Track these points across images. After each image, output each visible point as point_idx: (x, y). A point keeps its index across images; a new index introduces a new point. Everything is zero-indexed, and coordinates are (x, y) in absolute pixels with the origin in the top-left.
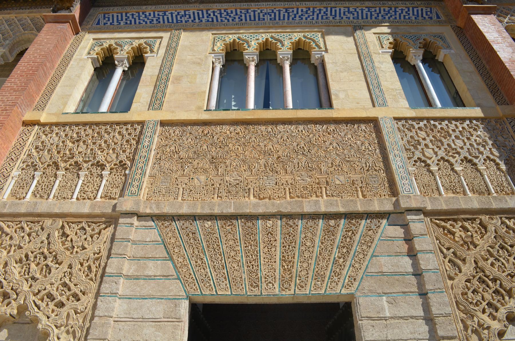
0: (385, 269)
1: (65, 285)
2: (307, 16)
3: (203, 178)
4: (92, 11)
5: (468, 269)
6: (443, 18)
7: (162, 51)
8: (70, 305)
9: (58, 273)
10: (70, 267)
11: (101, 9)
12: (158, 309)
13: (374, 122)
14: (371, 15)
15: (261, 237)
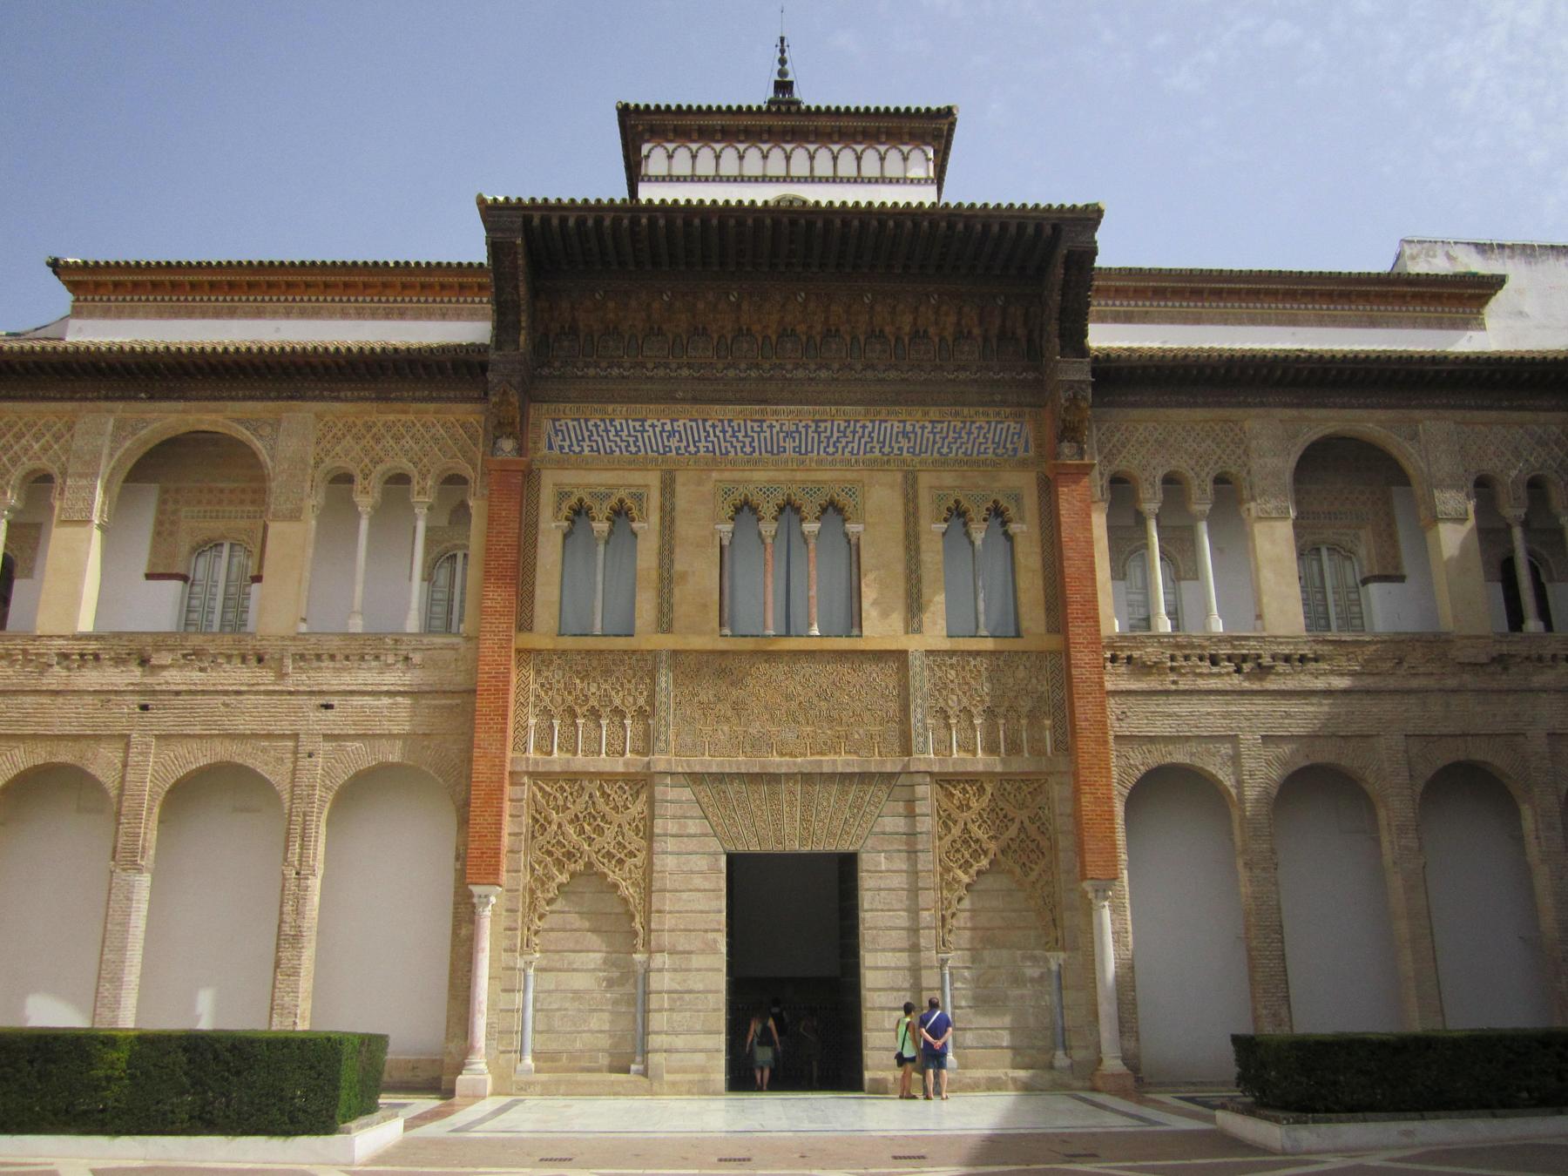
0: (887, 829)
1: (619, 843)
2: (844, 441)
3: (726, 728)
4: (532, 412)
5: (956, 831)
6: (1031, 453)
7: (655, 518)
8: (630, 862)
9: (610, 832)
10: (620, 826)
11: (545, 406)
12: (702, 863)
13: (901, 656)
14: (934, 442)
15: (784, 796)
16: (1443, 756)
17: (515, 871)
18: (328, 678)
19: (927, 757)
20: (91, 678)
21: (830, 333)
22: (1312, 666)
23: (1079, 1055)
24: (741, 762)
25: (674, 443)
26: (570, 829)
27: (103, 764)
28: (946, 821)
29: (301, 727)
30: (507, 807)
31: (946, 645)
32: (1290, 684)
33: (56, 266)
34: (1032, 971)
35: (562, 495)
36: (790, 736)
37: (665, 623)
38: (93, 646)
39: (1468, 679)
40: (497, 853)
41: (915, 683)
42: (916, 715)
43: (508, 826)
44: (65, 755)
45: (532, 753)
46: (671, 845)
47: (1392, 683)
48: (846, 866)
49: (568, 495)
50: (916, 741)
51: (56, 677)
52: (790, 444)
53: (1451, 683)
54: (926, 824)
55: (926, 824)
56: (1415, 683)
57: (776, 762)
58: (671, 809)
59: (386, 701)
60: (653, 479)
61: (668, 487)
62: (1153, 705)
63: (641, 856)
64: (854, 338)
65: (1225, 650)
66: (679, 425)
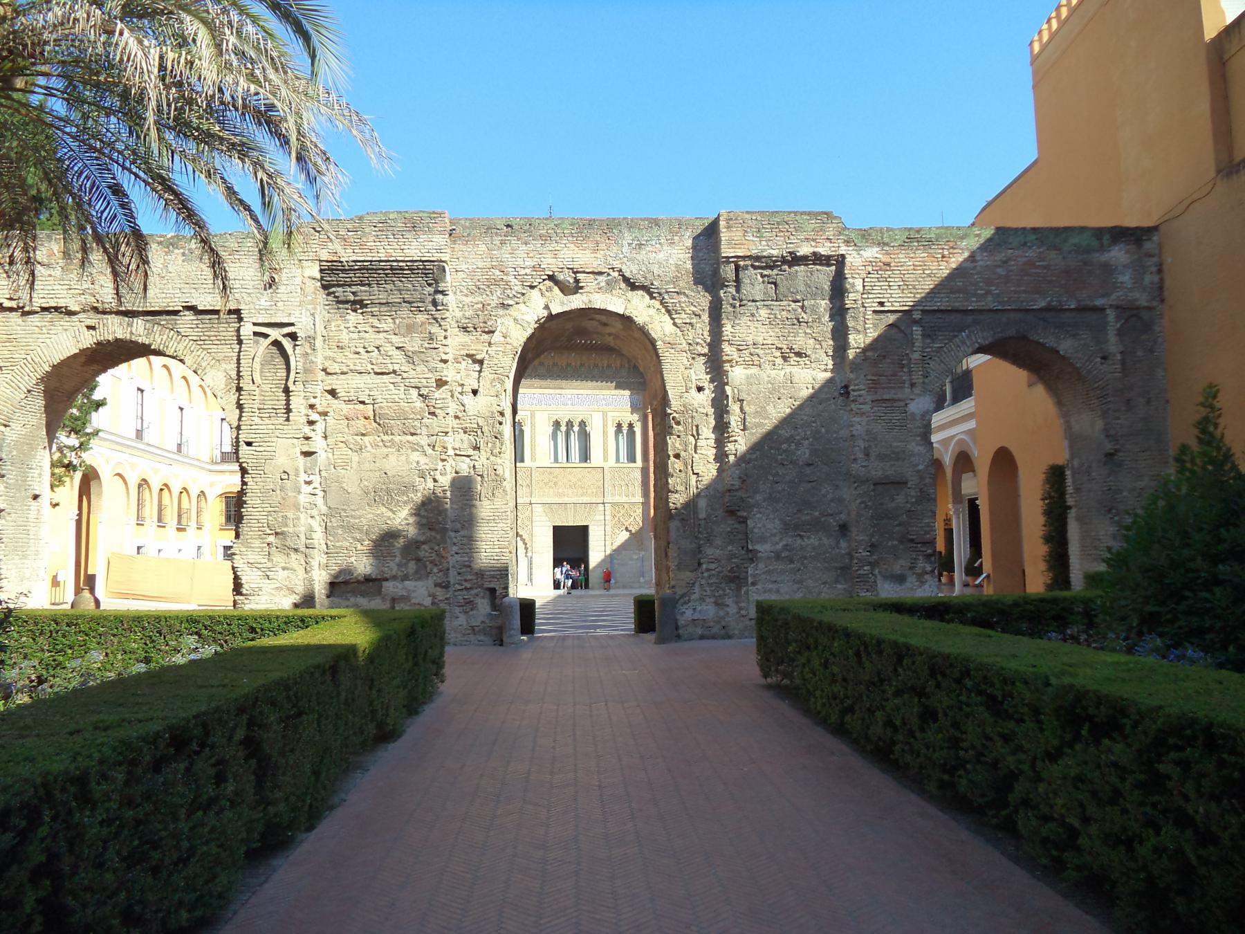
19: (608, 499)
21: (582, 365)
34: (635, 557)
48: (585, 529)
57: (566, 500)
61: (533, 416)
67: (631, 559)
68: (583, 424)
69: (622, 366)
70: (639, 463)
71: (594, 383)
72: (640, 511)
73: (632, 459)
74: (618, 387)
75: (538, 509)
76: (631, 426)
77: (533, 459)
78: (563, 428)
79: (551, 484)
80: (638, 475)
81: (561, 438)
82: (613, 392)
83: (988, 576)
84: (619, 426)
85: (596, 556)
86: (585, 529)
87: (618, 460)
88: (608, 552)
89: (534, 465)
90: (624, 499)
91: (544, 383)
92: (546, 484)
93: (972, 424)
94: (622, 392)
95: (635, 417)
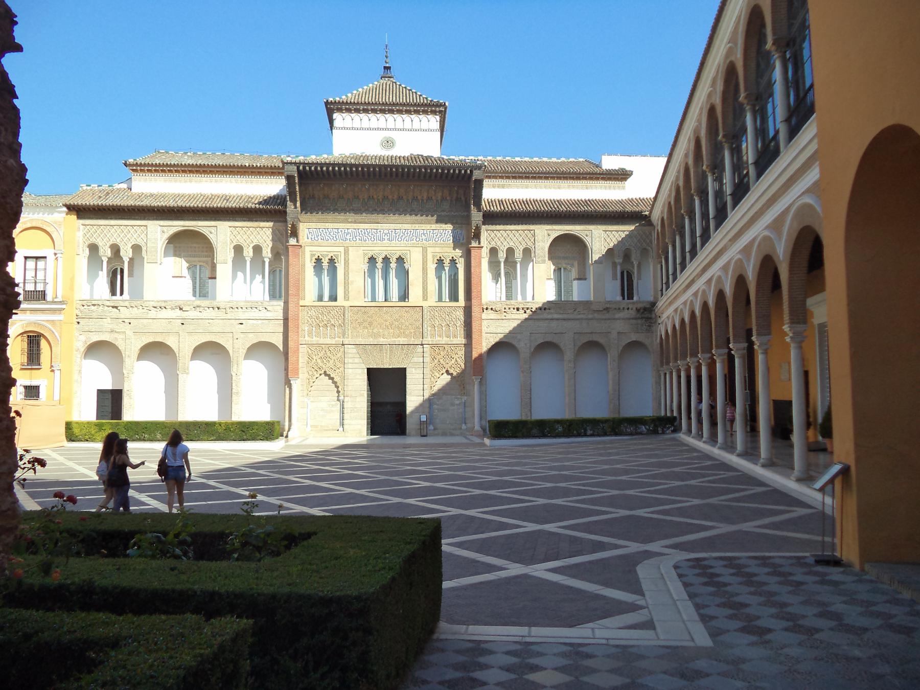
8: (337, 371)
12: (360, 371)
16: (585, 339)
17: (303, 373)
18: (241, 314)
19: (428, 340)
20: (164, 314)
21: (400, 198)
22: (547, 311)
23: (469, 425)
24: (371, 341)
25: (348, 237)
26: (319, 361)
27: (171, 342)
28: (434, 359)
29: (234, 330)
30: (300, 355)
31: (436, 304)
32: (541, 317)
33: (125, 164)
34: (457, 402)
35: (312, 255)
36: (386, 333)
37: (346, 298)
38: (163, 305)
39: (596, 315)
40: (298, 369)
41: (425, 317)
42: (425, 326)
43: (301, 360)
44: (159, 339)
45: (307, 338)
46: (350, 366)
47: (571, 316)
48: (404, 370)
49: (314, 255)
50: (425, 335)
51: (153, 313)
52: (386, 238)
53: (590, 316)
54: (427, 360)
55: (427, 359)
56: (579, 317)
57: (382, 340)
58: (350, 355)
59: (260, 322)
60: (342, 250)
61: (346, 252)
62: (498, 323)
63: (342, 369)
64: (408, 200)
65: (521, 306)
66: (350, 231)
67: (453, 405)
68: (400, 260)
69: (443, 199)
70: (462, 302)
71: (413, 217)
72: (461, 352)
73: (454, 297)
74: (438, 221)
75: (351, 350)
76: (453, 261)
77: (346, 298)
78: (379, 265)
79: (366, 324)
80: (460, 314)
81: (379, 274)
82: (434, 226)
83: (845, 472)
84: (440, 262)
85: (413, 401)
86: (404, 370)
87: (440, 299)
88: (427, 396)
89: (347, 304)
90: (444, 340)
91: (358, 217)
92: (360, 324)
93: (813, 175)
94: (444, 226)
95: (458, 252)
